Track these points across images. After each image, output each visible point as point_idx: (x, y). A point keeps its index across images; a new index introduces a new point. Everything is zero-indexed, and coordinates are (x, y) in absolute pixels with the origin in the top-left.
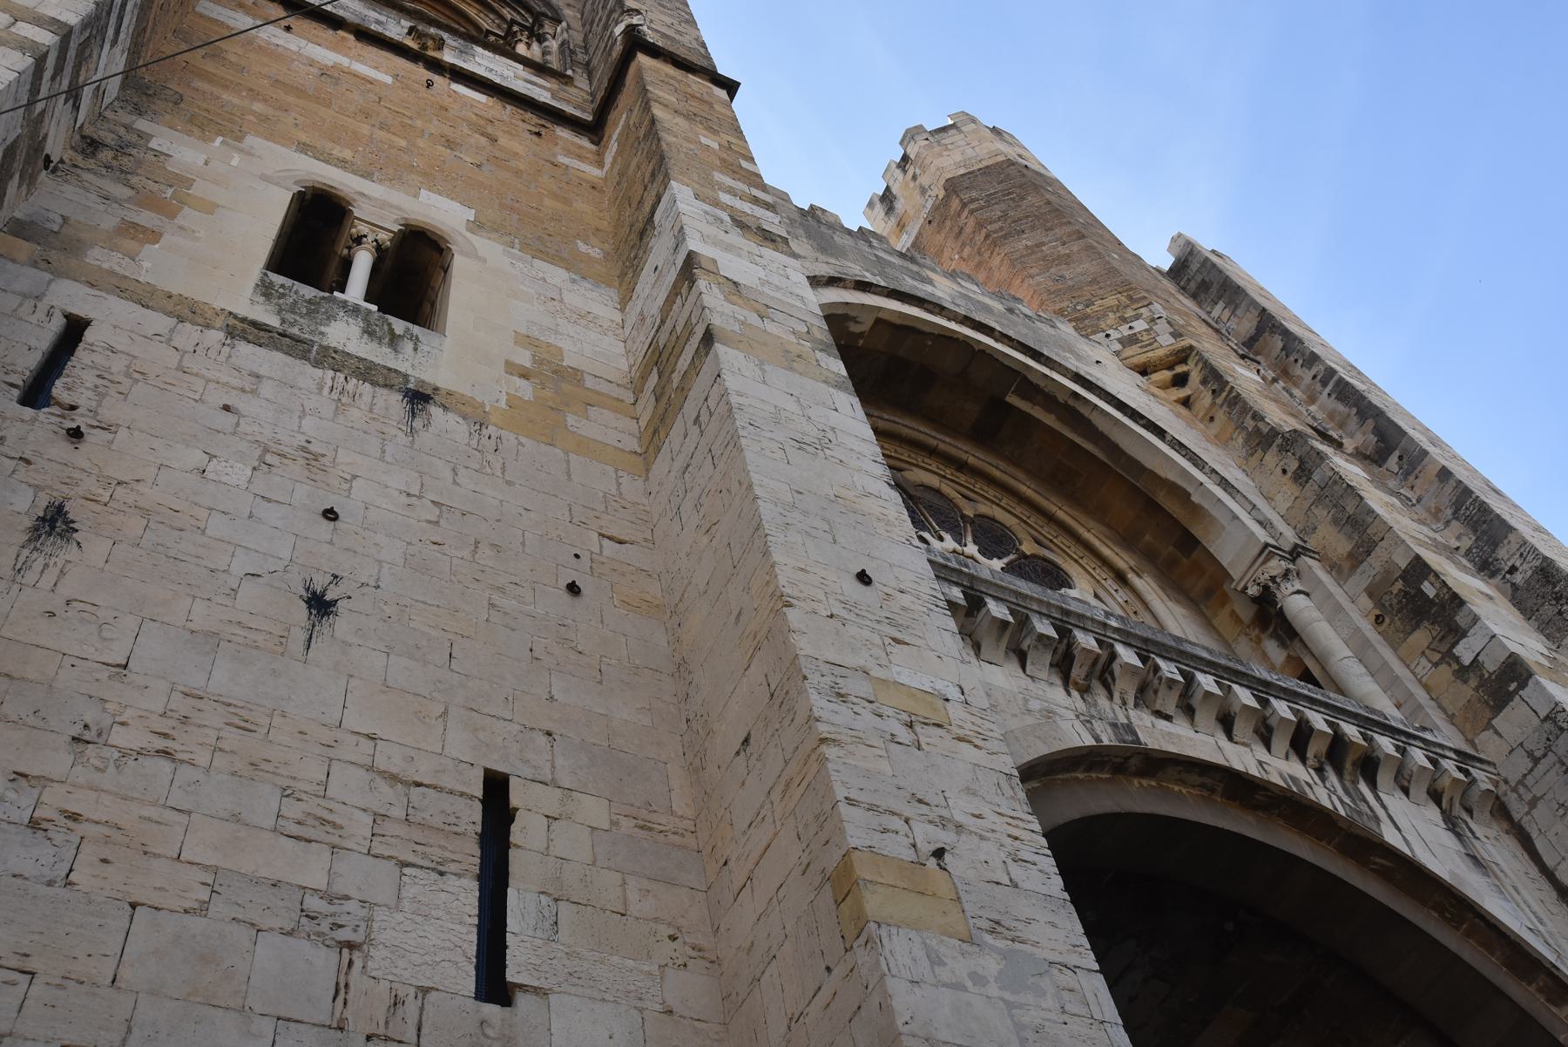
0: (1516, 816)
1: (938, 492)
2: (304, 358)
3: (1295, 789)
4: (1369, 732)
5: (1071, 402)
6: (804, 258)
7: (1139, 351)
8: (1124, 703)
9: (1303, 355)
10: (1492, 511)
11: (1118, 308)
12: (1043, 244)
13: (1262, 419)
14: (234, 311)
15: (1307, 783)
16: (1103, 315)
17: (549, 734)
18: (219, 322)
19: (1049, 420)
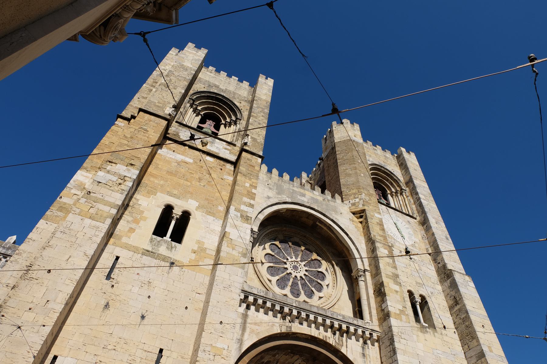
0: (380, 344)
1: (298, 243)
2: (154, 258)
3: (324, 339)
4: (349, 326)
5: (329, 226)
6: (272, 198)
7: (354, 208)
9: (416, 191)
10: (439, 247)
11: (355, 194)
12: (347, 169)
13: (371, 234)
14: (144, 248)
15: (329, 338)
16: (350, 195)
17: (173, 340)
18: (141, 252)
19: (325, 228)
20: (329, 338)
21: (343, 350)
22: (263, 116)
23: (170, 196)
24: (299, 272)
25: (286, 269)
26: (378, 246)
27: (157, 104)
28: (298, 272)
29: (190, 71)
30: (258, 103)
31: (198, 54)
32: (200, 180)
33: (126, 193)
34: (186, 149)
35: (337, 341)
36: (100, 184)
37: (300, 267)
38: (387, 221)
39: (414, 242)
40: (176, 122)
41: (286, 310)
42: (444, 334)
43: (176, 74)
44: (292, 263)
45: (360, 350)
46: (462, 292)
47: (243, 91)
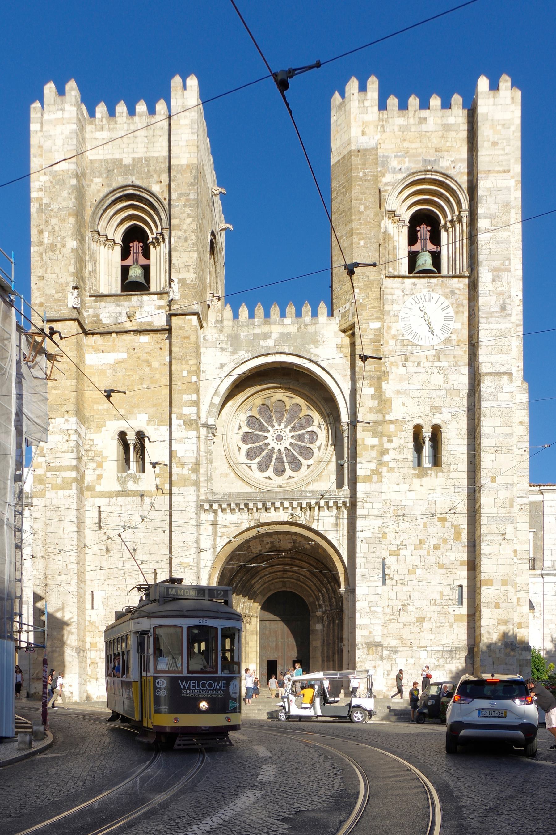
21: (314, 526)
35: (308, 519)
38: (408, 311)
39: (451, 333)
40: (90, 296)
42: (452, 469)
47: (161, 139)
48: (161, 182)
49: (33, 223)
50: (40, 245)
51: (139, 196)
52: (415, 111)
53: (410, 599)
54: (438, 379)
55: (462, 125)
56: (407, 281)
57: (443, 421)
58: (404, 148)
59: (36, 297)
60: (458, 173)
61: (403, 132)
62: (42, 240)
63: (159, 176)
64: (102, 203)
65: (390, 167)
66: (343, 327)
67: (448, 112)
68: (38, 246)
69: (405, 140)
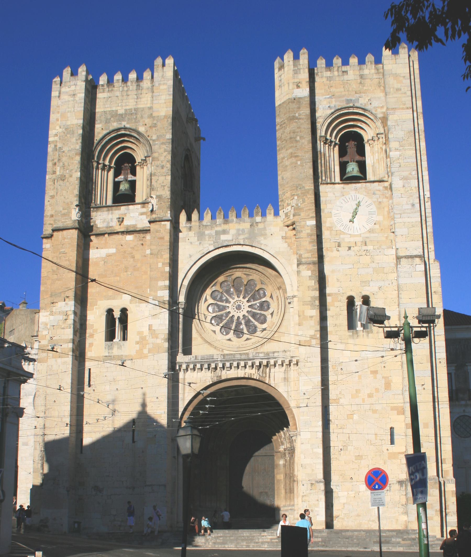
8: (221, 371)
12: (283, 158)
20: (254, 374)
22: (165, 151)
23: (107, 300)
24: (242, 311)
25: (229, 312)
26: (300, 270)
27: (64, 212)
28: (241, 312)
29: (77, 133)
30: (158, 130)
31: (78, 88)
32: (126, 269)
33: (72, 326)
34: (106, 238)
36: (55, 327)
37: (244, 304)
39: (375, 224)
41: (213, 365)
43: (65, 149)
44: (235, 304)
45: (282, 375)
46: (400, 285)
48: (146, 125)
49: (49, 158)
50: (54, 174)
51: (129, 134)
52: (339, 67)
53: (349, 440)
54: (366, 260)
55: (374, 75)
56: (337, 186)
57: (371, 292)
58: (331, 92)
59: (48, 211)
60: (374, 107)
61: (330, 81)
62: (55, 170)
63: (144, 121)
64: (102, 141)
65: (320, 107)
66: (287, 224)
67: (364, 67)
68: (52, 174)
69: (332, 87)
